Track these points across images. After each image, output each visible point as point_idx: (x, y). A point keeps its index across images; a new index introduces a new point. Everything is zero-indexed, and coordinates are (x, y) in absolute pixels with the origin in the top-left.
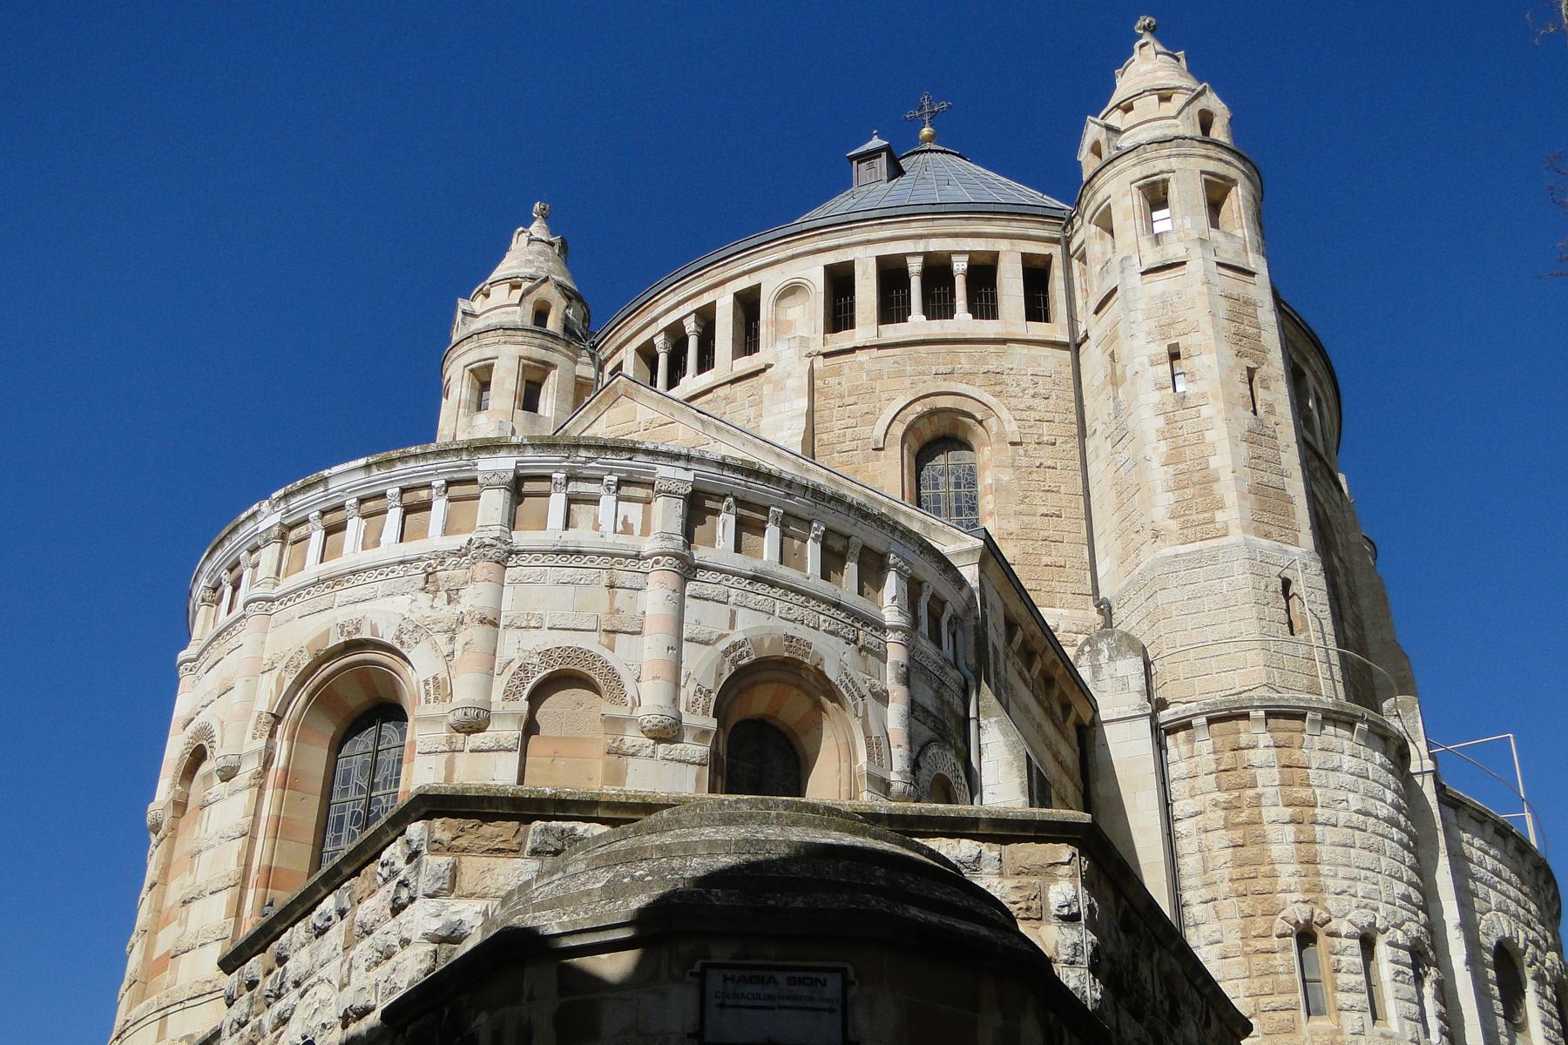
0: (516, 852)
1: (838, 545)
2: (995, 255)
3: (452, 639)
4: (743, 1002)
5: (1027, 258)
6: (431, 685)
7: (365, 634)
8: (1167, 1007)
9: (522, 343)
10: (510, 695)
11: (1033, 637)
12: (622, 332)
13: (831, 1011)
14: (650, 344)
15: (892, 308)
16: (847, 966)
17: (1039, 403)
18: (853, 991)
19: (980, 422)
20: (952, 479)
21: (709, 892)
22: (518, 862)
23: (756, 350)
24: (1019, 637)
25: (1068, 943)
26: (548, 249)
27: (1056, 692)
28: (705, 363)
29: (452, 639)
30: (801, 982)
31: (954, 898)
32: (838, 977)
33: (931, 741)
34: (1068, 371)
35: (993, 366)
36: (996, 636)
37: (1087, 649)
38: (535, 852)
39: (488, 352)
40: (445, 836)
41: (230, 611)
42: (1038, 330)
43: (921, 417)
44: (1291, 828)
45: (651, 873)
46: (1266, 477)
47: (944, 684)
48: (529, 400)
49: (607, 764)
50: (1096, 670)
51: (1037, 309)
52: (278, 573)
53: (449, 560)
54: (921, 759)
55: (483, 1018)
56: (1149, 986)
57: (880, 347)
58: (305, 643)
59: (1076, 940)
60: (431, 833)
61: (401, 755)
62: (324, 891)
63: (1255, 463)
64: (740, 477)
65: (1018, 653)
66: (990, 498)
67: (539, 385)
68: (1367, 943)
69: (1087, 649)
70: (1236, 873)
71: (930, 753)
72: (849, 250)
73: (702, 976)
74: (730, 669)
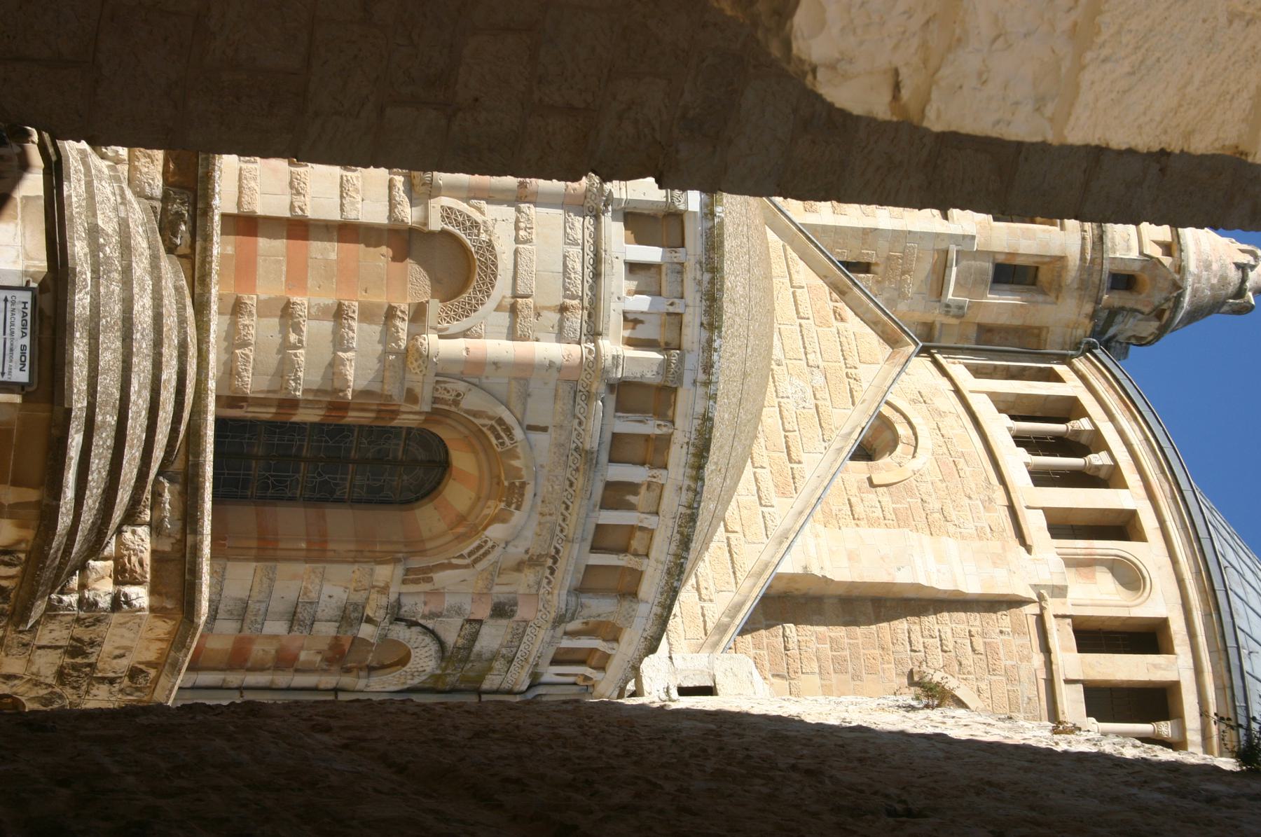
9: (1083, 258)
10: (448, 213)
12: (1102, 380)
14: (1082, 413)
16: (35, 387)
21: (87, 293)
26: (1231, 289)
28: (1041, 478)
30: (23, 354)
31: (95, 474)
47: (511, 662)
49: (379, 306)
54: (419, 629)
59: (101, 605)
64: (693, 436)
67: (1034, 284)
71: (428, 639)
72: (1188, 649)
74: (484, 426)
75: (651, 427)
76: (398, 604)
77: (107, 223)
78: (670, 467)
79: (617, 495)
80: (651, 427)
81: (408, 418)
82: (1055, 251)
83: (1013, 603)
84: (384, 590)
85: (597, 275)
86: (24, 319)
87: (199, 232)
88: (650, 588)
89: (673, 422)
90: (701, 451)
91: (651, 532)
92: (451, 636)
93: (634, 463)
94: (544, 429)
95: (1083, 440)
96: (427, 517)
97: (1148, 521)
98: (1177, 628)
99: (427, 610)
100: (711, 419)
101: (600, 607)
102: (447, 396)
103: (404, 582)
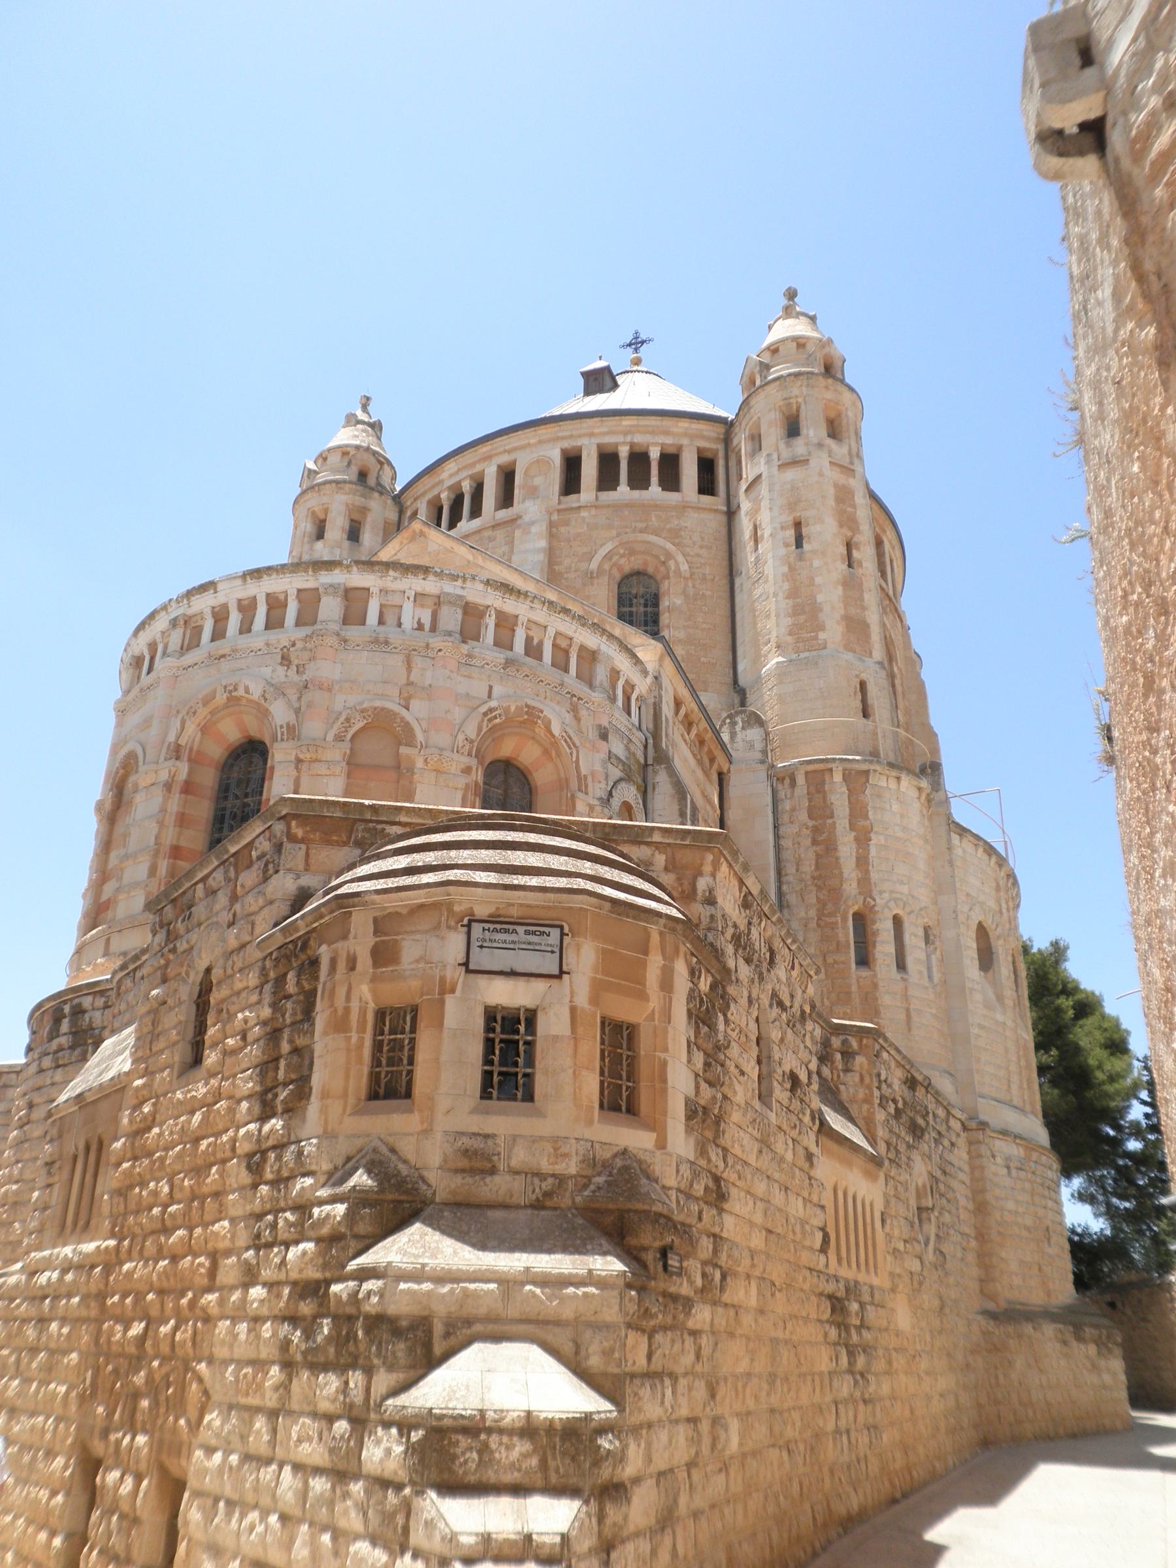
0: (345, 844)
1: (563, 644)
2: (680, 448)
3: (299, 698)
4: (495, 945)
5: (699, 450)
6: (285, 729)
7: (241, 692)
8: (768, 955)
10: (339, 738)
11: (692, 712)
13: (552, 952)
14: (438, 497)
15: (607, 480)
17: (703, 552)
18: (567, 940)
19: (664, 563)
20: (642, 601)
22: (346, 849)
23: (512, 505)
24: (682, 712)
25: (708, 914)
27: (706, 749)
28: (476, 512)
29: (299, 698)
30: (534, 933)
32: (558, 930)
33: (620, 780)
34: (724, 531)
35: (675, 523)
36: (667, 710)
37: (728, 721)
38: (359, 844)
39: (325, 499)
40: (300, 833)
41: (149, 671)
42: (706, 499)
43: (622, 556)
44: (854, 846)
45: (436, 859)
46: (853, 611)
48: (354, 535)
50: (733, 735)
51: (707, 486)
52: (182, 648)
53: (299, 645)
55: (324, 948)
56: (757, 944)
57: (596, 507)
58: (200, 696)
60: (289, 827)
61: (264, 774)
62: (216, 863)
63: (846, 601)
65: (682, 722)
66: (667, 615)
68: (897, 921)
69: (728, 721)
70: (816, 874)
73: (469, 926)
75: (490, 621)
76: (601, 799)
77: (402, 862)
78: (517, 613)
79: (533, 650)
80: (490, 621)
81: (478, 776)
82: (343, 508)
83: (551, 525)
84: (591, 808)
85: (387, 643)
86: (500, 931)
87: (392, 818)
88: (591, 640)
89: (488, 607)
90: (507, 589)
91: (558, 634)
92: (616, 773)
93: (513, 636)
94: (491, 687)
95: (453, 496)
96: (542, 777)
97: (504, 459)
98: (566, 444)
99: (604, 782)
100: (488, 581)
101: (601, 674)
102: (467, 747)
103: (587, 793)
